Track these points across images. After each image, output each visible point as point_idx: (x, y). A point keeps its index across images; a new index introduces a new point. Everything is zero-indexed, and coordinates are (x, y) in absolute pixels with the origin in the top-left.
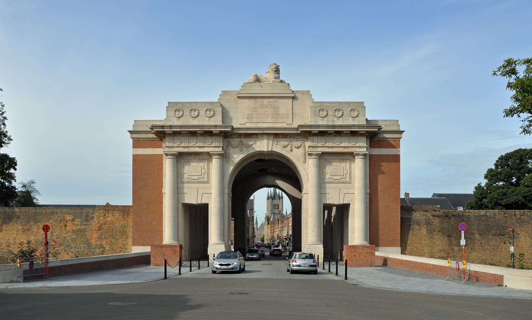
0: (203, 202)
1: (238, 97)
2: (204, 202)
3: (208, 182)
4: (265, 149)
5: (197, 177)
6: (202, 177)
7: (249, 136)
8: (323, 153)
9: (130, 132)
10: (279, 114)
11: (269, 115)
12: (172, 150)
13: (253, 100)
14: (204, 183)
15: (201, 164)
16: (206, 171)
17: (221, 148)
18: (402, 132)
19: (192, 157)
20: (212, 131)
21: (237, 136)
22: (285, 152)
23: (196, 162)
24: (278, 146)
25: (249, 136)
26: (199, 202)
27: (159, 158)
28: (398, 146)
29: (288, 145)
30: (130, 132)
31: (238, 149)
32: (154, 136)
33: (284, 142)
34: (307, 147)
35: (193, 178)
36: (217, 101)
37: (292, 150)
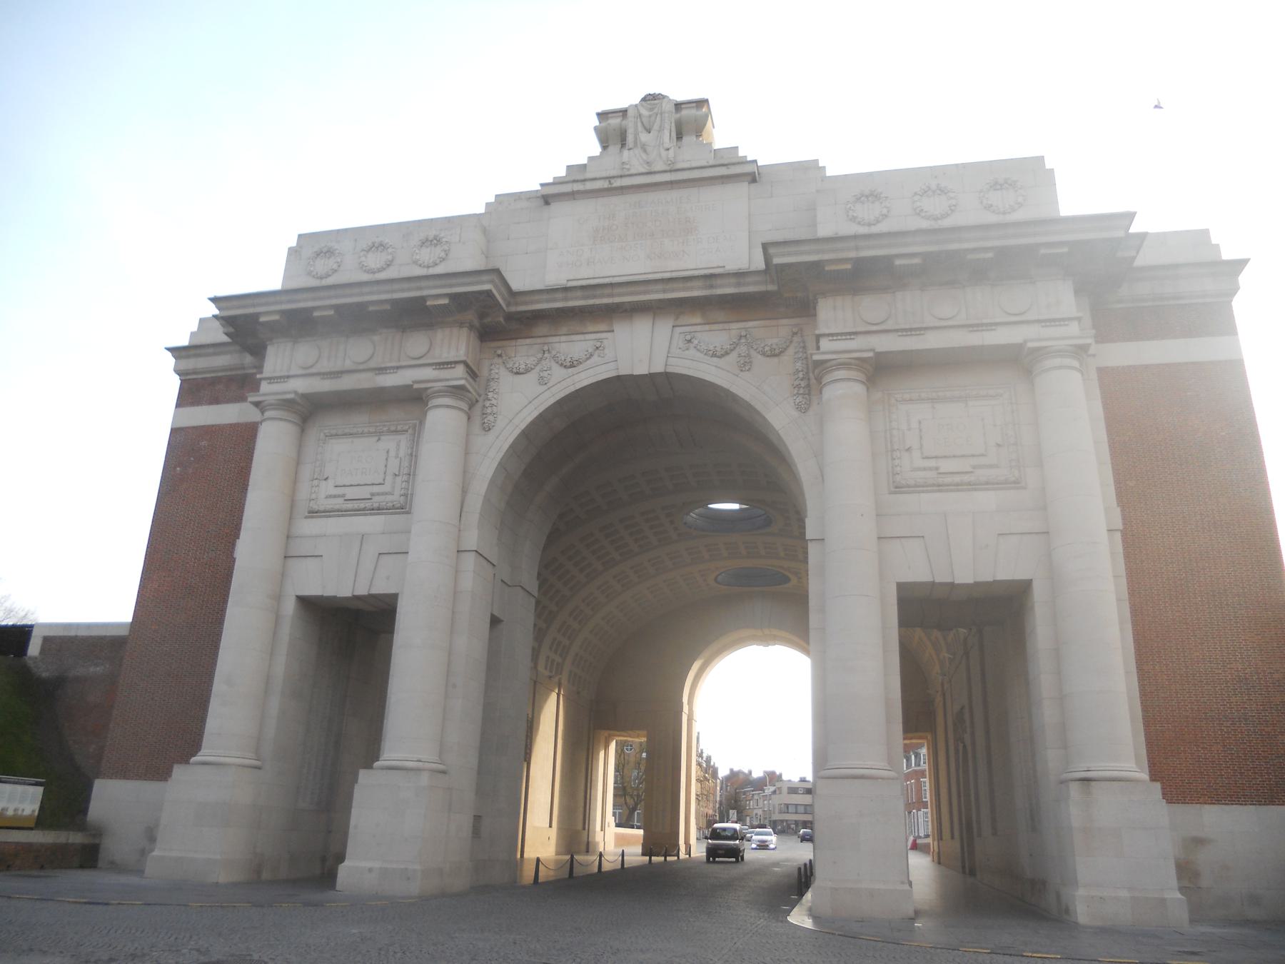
2: (381, 588)
3: (404, 508)
4: (641, 370)
5: (364, 492)
9: (173, 350)
15: (388, 443)
16: (406, 464)
17: (460, 371)
24: (692, 352)
26: (362, 590)
30: (173, 350)
33: (717, 337)
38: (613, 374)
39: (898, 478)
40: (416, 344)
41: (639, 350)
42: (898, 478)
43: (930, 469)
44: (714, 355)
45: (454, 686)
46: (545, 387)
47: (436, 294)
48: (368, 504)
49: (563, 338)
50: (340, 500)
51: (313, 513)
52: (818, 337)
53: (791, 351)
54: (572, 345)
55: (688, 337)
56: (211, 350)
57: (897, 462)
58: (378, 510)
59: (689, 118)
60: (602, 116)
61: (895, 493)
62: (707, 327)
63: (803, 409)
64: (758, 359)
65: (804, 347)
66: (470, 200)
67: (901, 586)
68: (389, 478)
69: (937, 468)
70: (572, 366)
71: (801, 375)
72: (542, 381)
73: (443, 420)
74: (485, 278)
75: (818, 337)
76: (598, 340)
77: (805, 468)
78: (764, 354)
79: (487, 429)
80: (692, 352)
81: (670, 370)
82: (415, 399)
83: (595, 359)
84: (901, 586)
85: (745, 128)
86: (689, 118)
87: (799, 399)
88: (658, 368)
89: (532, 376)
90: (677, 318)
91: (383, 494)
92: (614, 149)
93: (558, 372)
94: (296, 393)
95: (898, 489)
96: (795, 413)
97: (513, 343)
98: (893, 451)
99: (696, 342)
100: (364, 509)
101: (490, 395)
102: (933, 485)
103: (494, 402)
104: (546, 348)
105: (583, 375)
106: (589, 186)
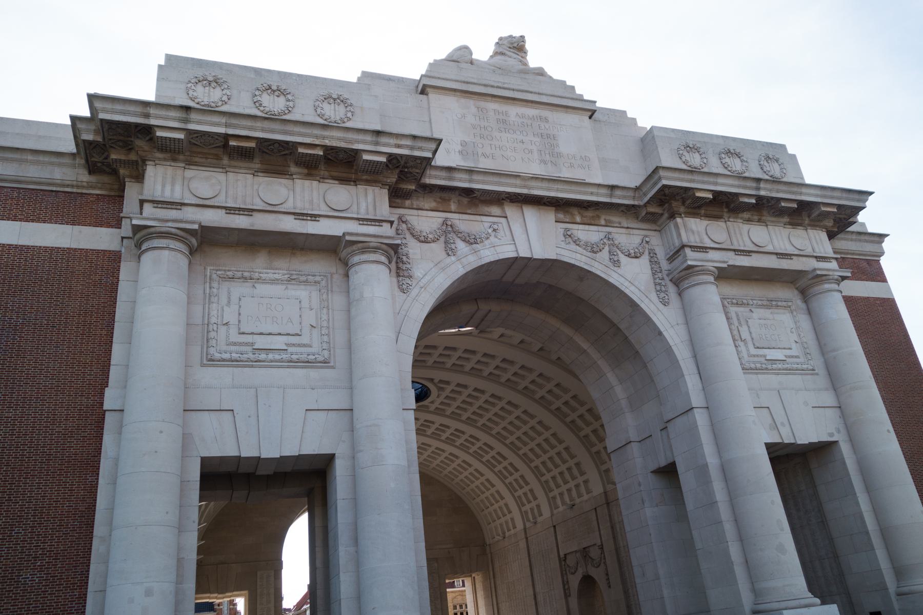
0: (310, 448)
6: (305, 340)
7: (474, 199)
10: (559, 155)
11: (531, 152)
12: (173, 214)
13: (471, 103)
14: (308, 363)
18: (882, 237)
19: (259, 264)
20: (357, 152)
21: (433, 205)
22: (598, 266)
23: (274, 282)
25: (474, 199)
27: (103, 272)
28: (878, 276)
29: (604, 244)
31: (437, 248)
32: (84, 176)
33: (590, 234)
35: (261, 342)
37: (617, 263)
40: (340, 195)
47: (374, 152)
48: (285, 356)
50: (249, 349)
51: (211, 361)
56: (54, 159)
58: (294, 363)
64: (623, 259)
66: (344, 69)
68: (306, 331)
73: (373, 277)
76: (494, 223)
78: (629, 256)
82: (335, 249)
91: (299, 345)
94: (200, 224)
96: (661, 306)
100: (281, 361)
101: (404, 258)
103: (408, 266)
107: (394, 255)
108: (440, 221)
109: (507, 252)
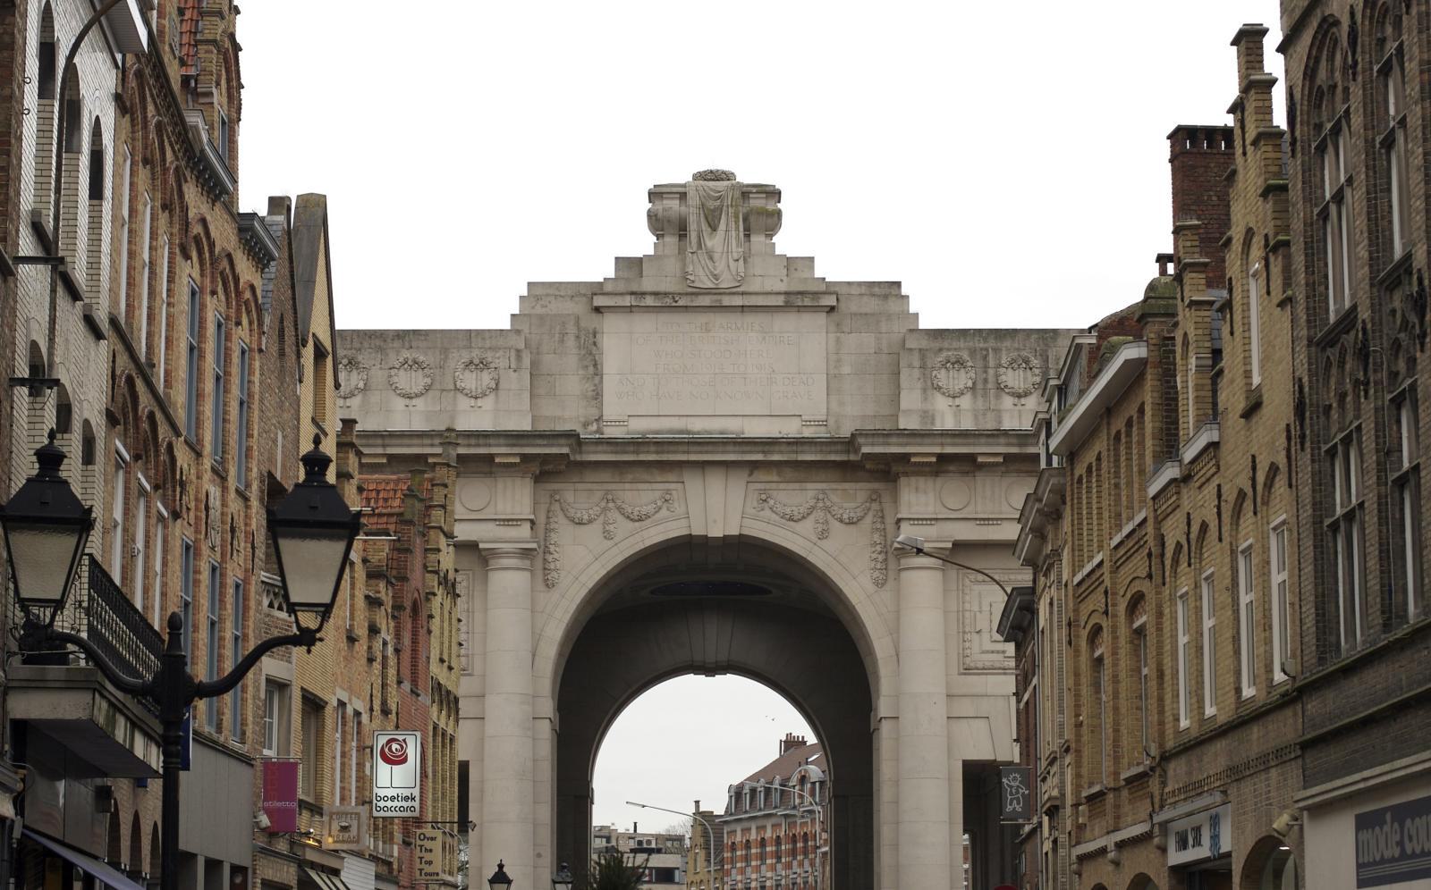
1: (598, 310)
4: (716, 532)
8: (959, 546)
22: (796, 539)
34: (890, 521)
36: (507, 325)
38: (685, 532)
39: (968, 660)
41: (717, 510)
42: (968, 660)
43: (998, 652)
44: (791, 519)
45: (539, 855)
46: (610, 543)
49: (627, 486)
52: (899, 520)
53: (869, 519)
54: (641, 495)
55: (764, 497)
57: (967, 644)
59: (757, 209)
60: (655, 194)
61: (965, 674)
62: (782, 486)
63: (880, 584)
65: (883, 517)
67: (964, 761)
69: (1004, 652)
70: (639, 520)
71: (878, 548)
72: (607, 535)
74: (563, 441)
75: (899, 520)
77: (881, 646)
78: (841, 521)
79: (549, 585)
80: (767, 513)
81: (746, 532)
83: (664, 512)
84: (964, 761)
85: (826, 237)
86: (757, 209)
87: (877, 574)
88: (735, 532)
89: (596, 528)
90: (750, 475)
92: (671, 240)
93: (622, 527)
95: (967, 670)
96: (871, 587)
97: (570, 486)
98: (964, 632)
99: (772, 502)
101: (552, 548)
102: (1000, 669)
103: (556, 556)
104: (610, 497)
105: (653, 531)
106: (649, 301)
107: (536, 557)
108: (603, 493)
109: (675, 530)
